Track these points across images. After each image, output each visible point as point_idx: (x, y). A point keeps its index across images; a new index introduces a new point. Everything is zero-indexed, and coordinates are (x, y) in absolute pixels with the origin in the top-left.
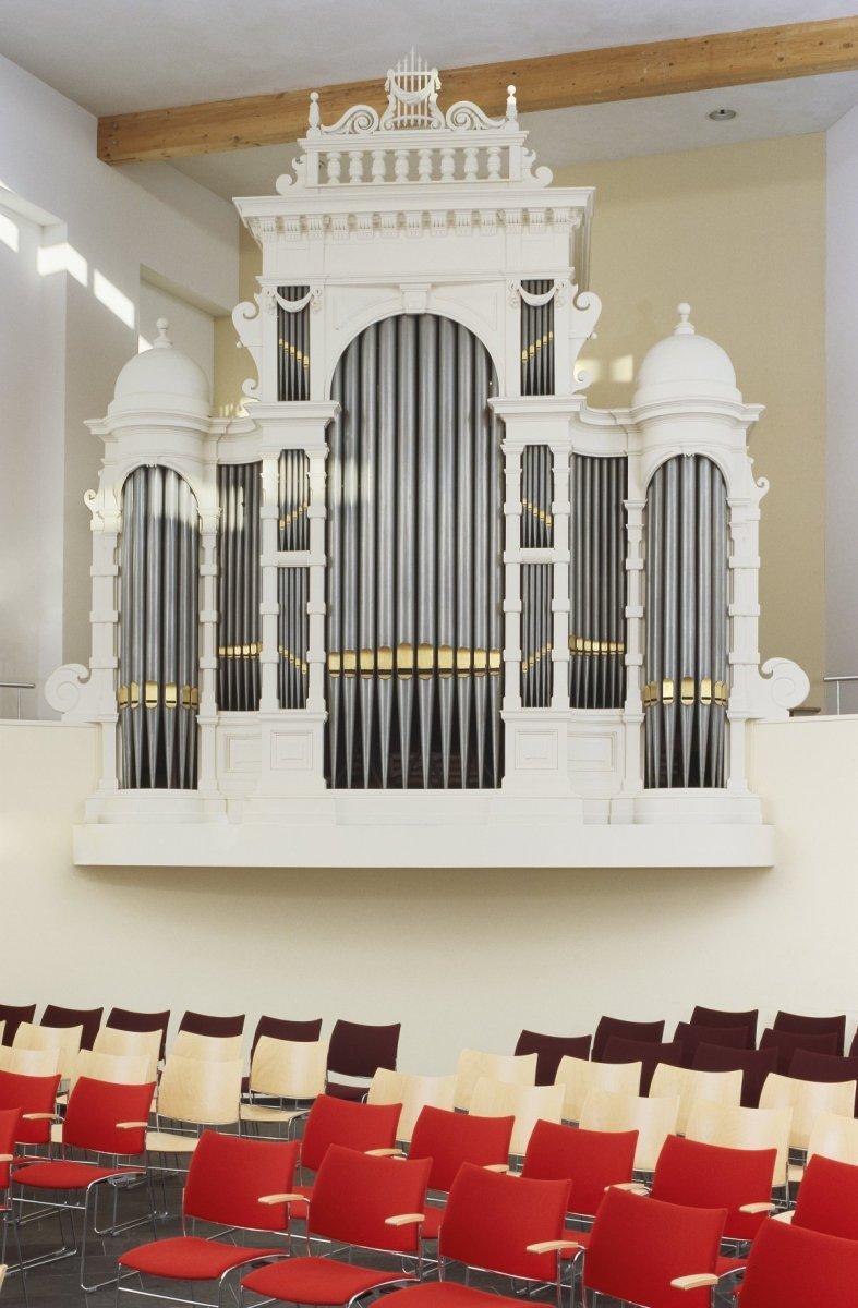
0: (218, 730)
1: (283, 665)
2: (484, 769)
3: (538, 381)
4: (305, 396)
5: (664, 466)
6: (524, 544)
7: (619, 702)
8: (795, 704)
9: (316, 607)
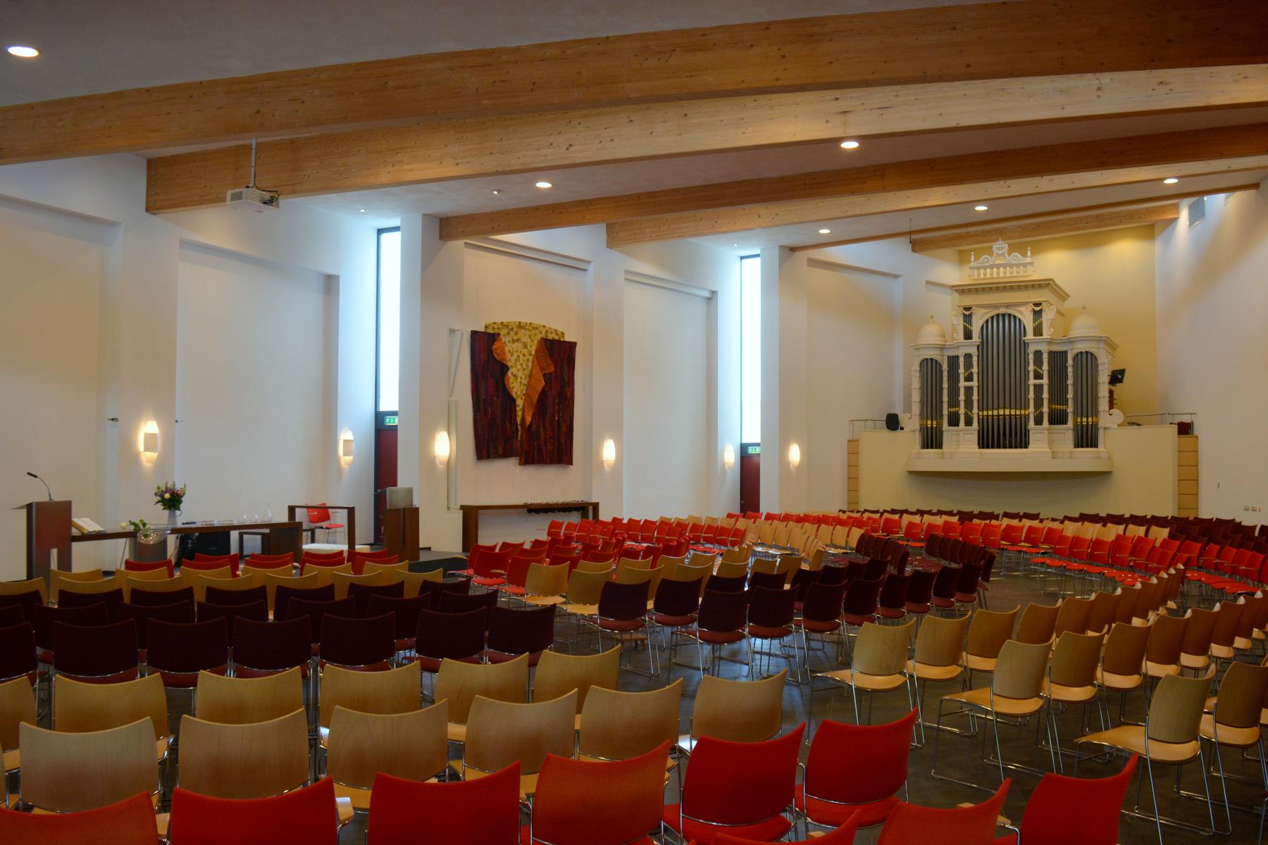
0: (948, 432)
1: (966, 414)
2: (1024, 444)
3: (1038, 331)
4: (971, 338)
5: (1077, 354)
6: (1035, 378)
7: (1065, 422)
8: (1119, 423)
9: (975, 397)
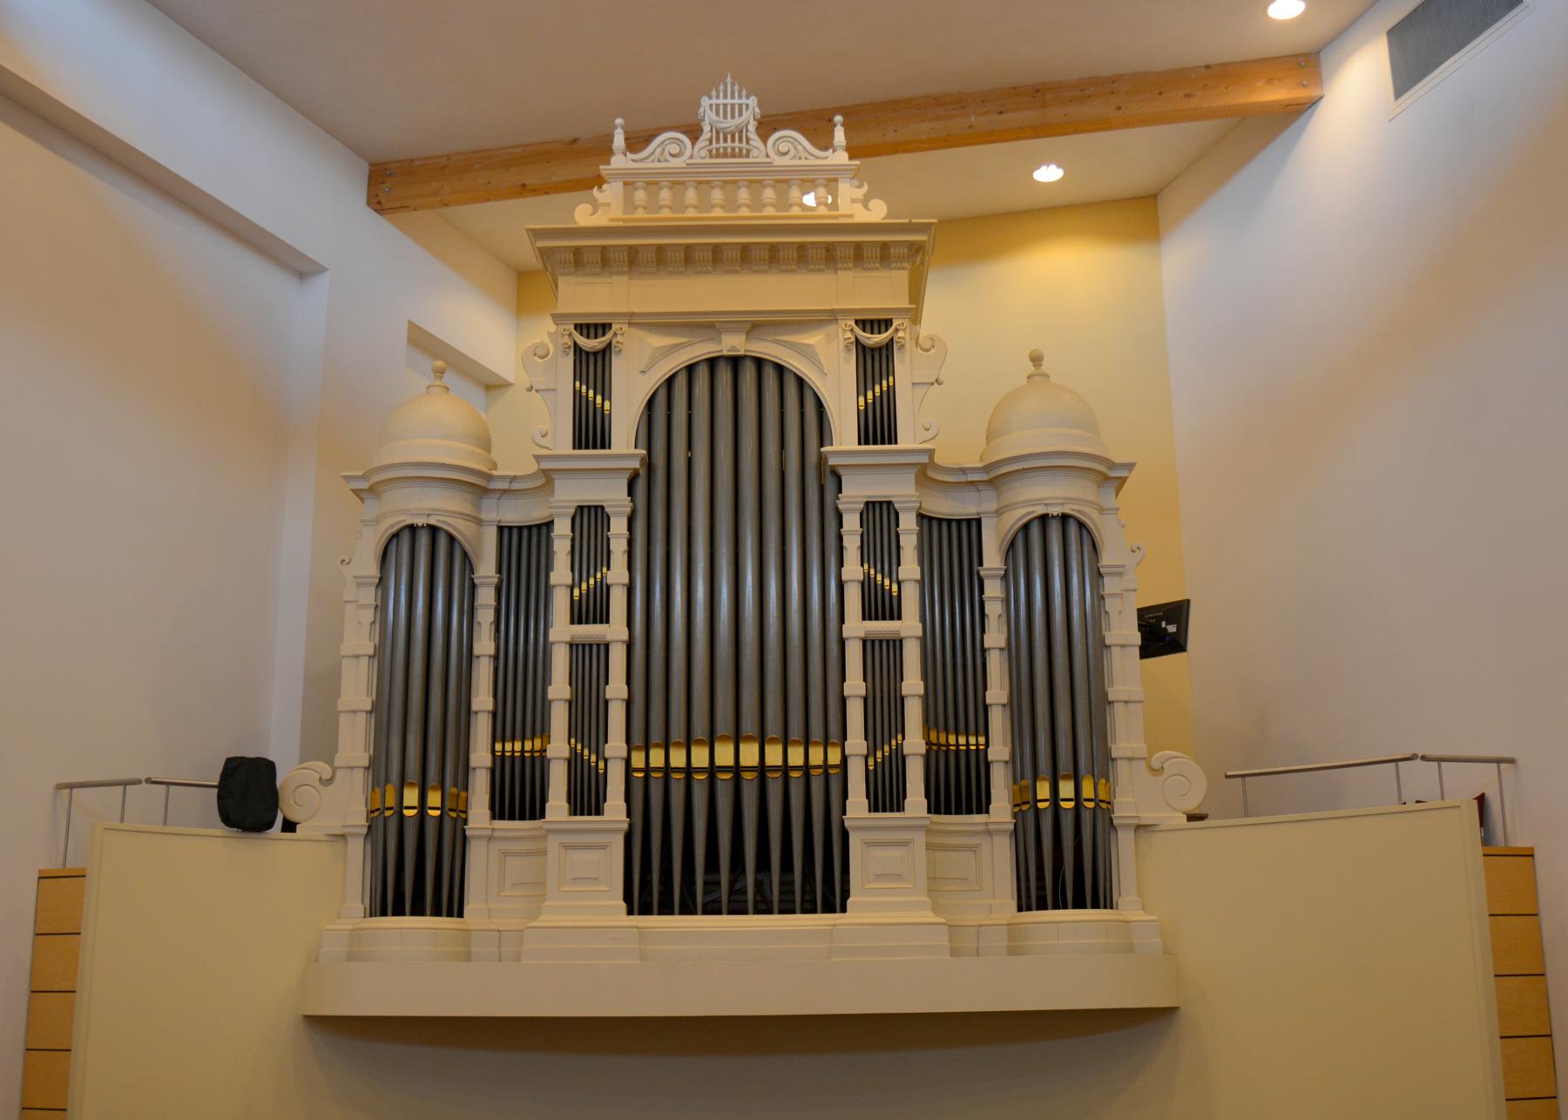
1: (574, 762)
4: (605, 443)
5: (1026, 527)
6: (867, 615)
7: (982, 806)
9: (616, 689)
